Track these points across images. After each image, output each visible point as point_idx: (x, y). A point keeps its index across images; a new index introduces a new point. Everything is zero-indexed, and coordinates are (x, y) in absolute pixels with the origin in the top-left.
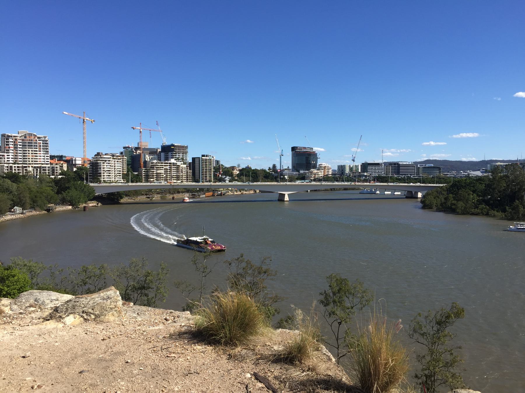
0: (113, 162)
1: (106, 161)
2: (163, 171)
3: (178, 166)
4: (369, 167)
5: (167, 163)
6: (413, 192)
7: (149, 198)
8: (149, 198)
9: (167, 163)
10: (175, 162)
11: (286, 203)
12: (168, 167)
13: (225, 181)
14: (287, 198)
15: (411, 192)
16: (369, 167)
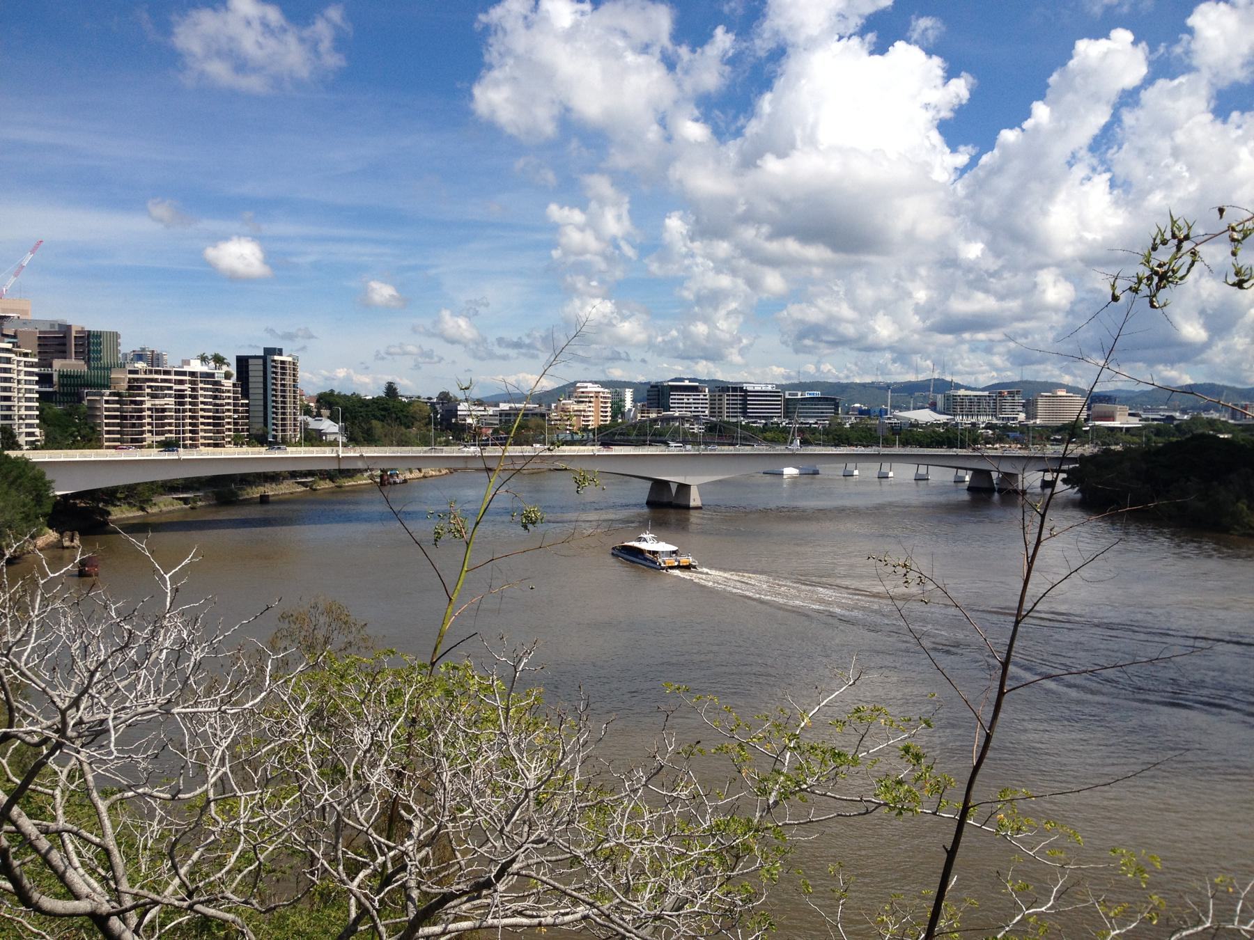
2: (170, 402)
4: (675, 396)
5: (184, 373)
7: (185, 501)
8: (185, 501)
11: (692, 512)
12: (187, 386)
14: (695, 499)
15: (988, 473)
16: (675, 396)
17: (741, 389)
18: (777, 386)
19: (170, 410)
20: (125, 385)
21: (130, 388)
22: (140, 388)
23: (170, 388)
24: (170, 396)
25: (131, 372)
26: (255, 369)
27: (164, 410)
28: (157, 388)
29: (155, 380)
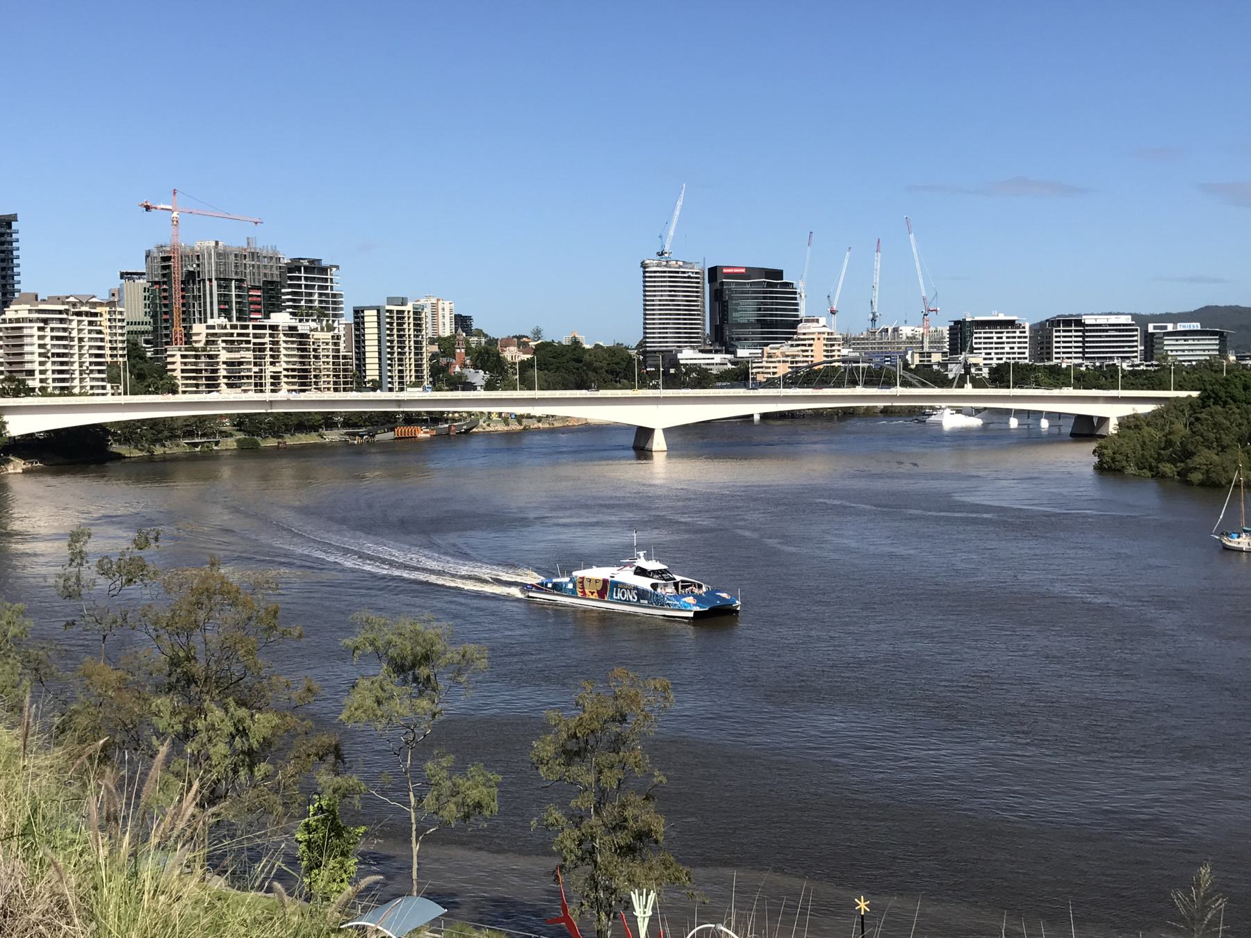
0: (74, 325)
1: (45, 321)
3: (302, 336)
4: (979, 337)
5: (263, 327)
6: (1095, 421)
8: (196, 445)
9: (263, 327)
10: (294, 323)
13: (471, 387)
14: (659, 443)
16: (979, 337)
17: (1079, 323)
18: (1134, 316)
19: (249, 363)
20: (203, 338)
21: (207, 342)
22: (214, 342)
23: (249, 342)
24: (248, 349)
25: (208, 327)
26: (370, 318)
27: (241, 363)
28: (232, 342)
29: (232, 335)
